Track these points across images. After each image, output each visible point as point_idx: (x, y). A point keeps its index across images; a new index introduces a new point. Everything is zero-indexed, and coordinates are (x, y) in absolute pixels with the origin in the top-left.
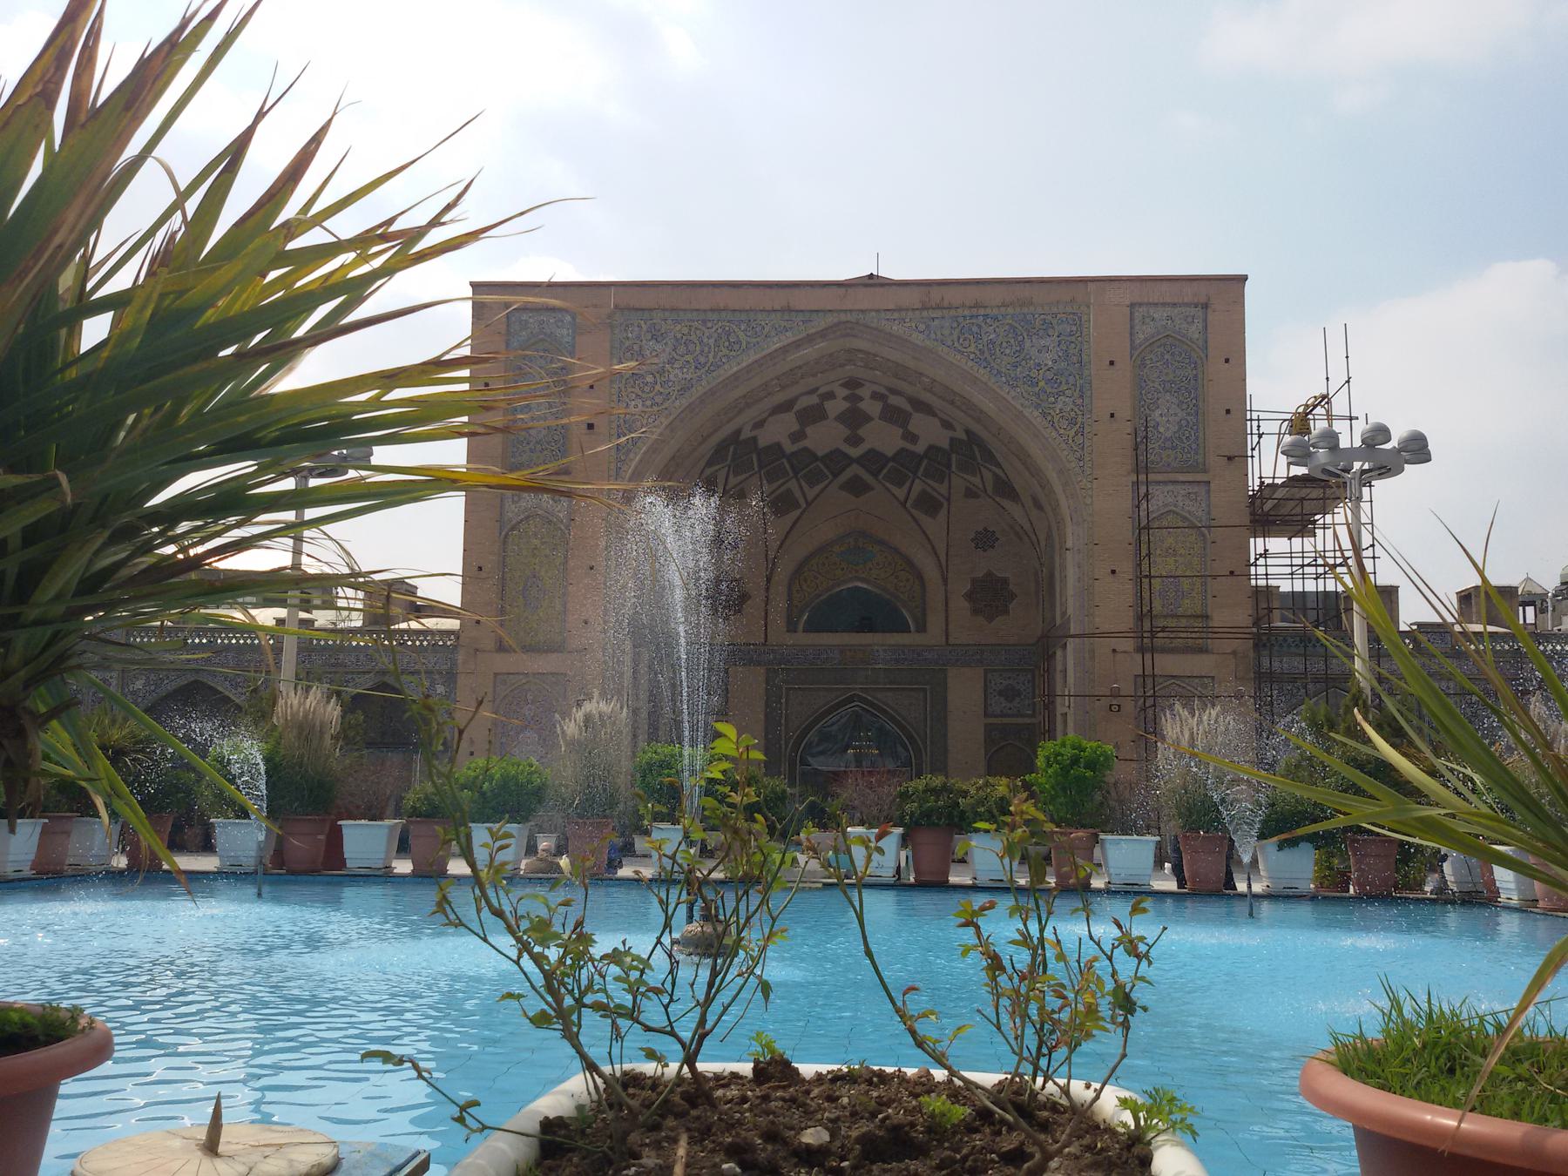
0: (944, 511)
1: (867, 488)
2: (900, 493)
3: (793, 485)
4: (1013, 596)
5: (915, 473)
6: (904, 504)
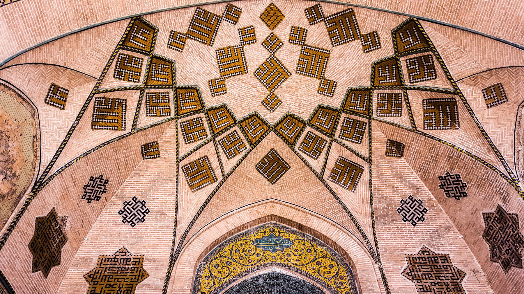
0: (365, 175)
1: (284, 167)
2: (317, 164)
3: (209, 150)
4: (461, 275)
5: (331, 135)
6: (320, 178)
